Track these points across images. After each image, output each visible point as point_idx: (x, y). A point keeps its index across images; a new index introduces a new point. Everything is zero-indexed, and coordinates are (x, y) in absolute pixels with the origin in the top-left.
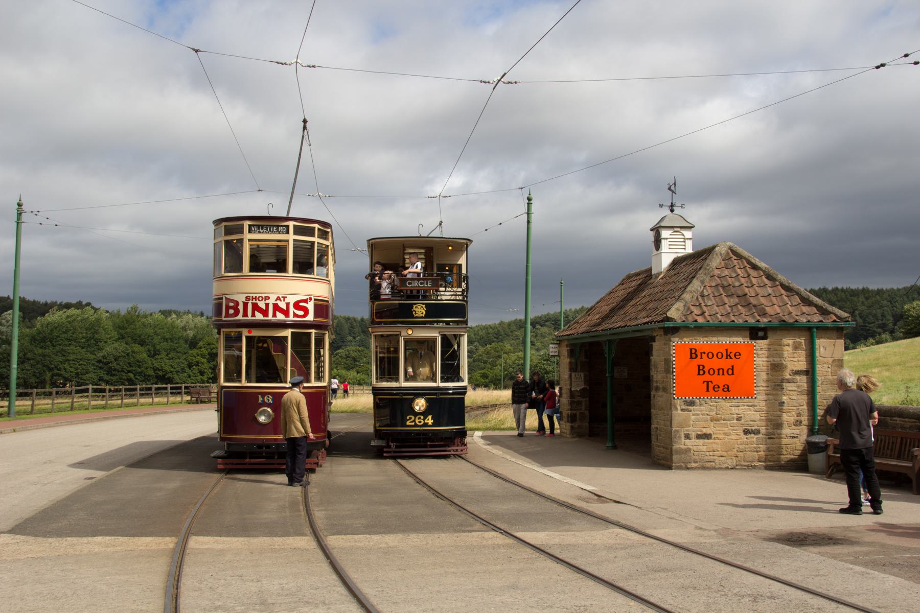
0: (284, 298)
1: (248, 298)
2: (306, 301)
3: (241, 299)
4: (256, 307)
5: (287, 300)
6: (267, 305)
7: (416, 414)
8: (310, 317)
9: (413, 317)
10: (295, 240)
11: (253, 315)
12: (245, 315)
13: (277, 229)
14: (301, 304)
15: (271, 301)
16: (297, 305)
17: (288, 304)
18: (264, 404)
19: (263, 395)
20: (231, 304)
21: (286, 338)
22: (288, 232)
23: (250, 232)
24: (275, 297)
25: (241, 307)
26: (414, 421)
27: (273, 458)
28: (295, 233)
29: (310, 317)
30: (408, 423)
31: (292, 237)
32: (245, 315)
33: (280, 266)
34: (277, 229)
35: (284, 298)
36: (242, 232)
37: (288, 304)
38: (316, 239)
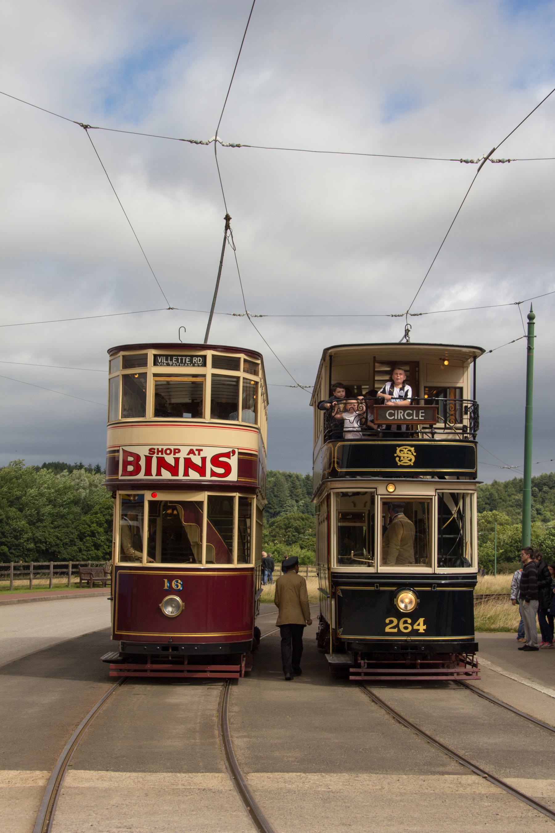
1: (152, 451)
2: (227, 455)
3: (143, 452)
4: (162, 463)
5: (203, 454)
6: (177, 460)
7: (400, 615)
8: (233, 477)
9: (396, 466)
10: (213, 375)
11: (159, 473)
12: (148, 472)
13: (191, 361)
14: (221, 459)
15: (183, 455)
16: (215, 461)
17: (204, 460)
18: (171, 591)
19: (171, 578)
20: (130, 459)
21: (201, 503)
22: (204, 365)
23: (155, 364)
24: (188, 448)
25: (143, 463)
26: (397, 626)
27: (182, 663)
28: (214, 366)
29: (233, 477)
30: (387, 629)
31: (209, 371)
32: (148, 472)
33: (195, 409)
34: (191, 361)
35: (199, 451)
36: (145, 364)
37: (204, 460)
38: (241, 374)
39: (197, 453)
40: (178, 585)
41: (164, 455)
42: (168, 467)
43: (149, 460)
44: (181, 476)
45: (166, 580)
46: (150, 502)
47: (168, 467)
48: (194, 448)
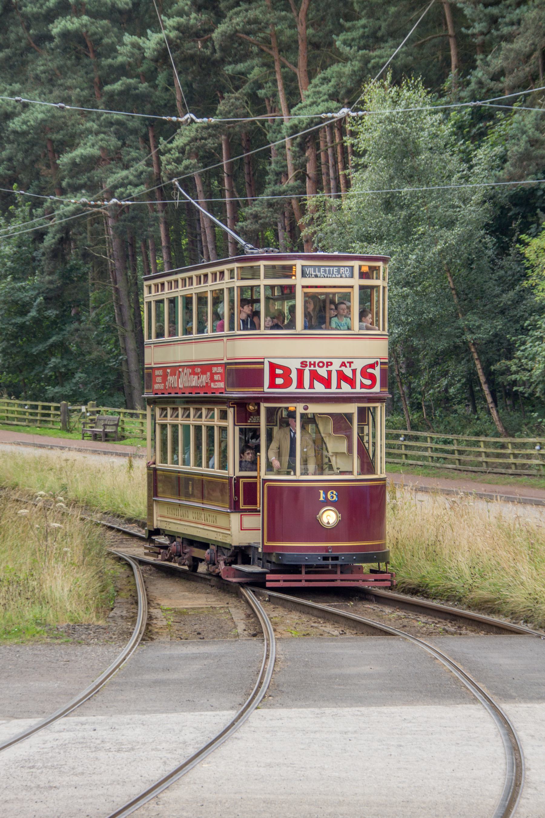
0: (350, 363)
1: (304, 364)
2: (372, 366)
3: (294, 365)
4: (314, 376)
6: (329, 373)
11: (312, 386)
12: (300, 385)
13: (338, 271)
16: (364, 373)
17: (354, 371)
18: (327, 503)
19: (326, 490)
24: (340, 361)
25: (294, 376)
29: (377, 389)
32: (300, 385)
34: (338, 271)
35: (350, 363)
37: (354, 371)
39: (348, 365)
40: (333, 496)
41: (317, 368)
42: (321, 379)
43: (300, 373)
44: (334, 389)
45: (322, 492)
46: (302, 415)
47: (321, 379)
48: (346, 361)
